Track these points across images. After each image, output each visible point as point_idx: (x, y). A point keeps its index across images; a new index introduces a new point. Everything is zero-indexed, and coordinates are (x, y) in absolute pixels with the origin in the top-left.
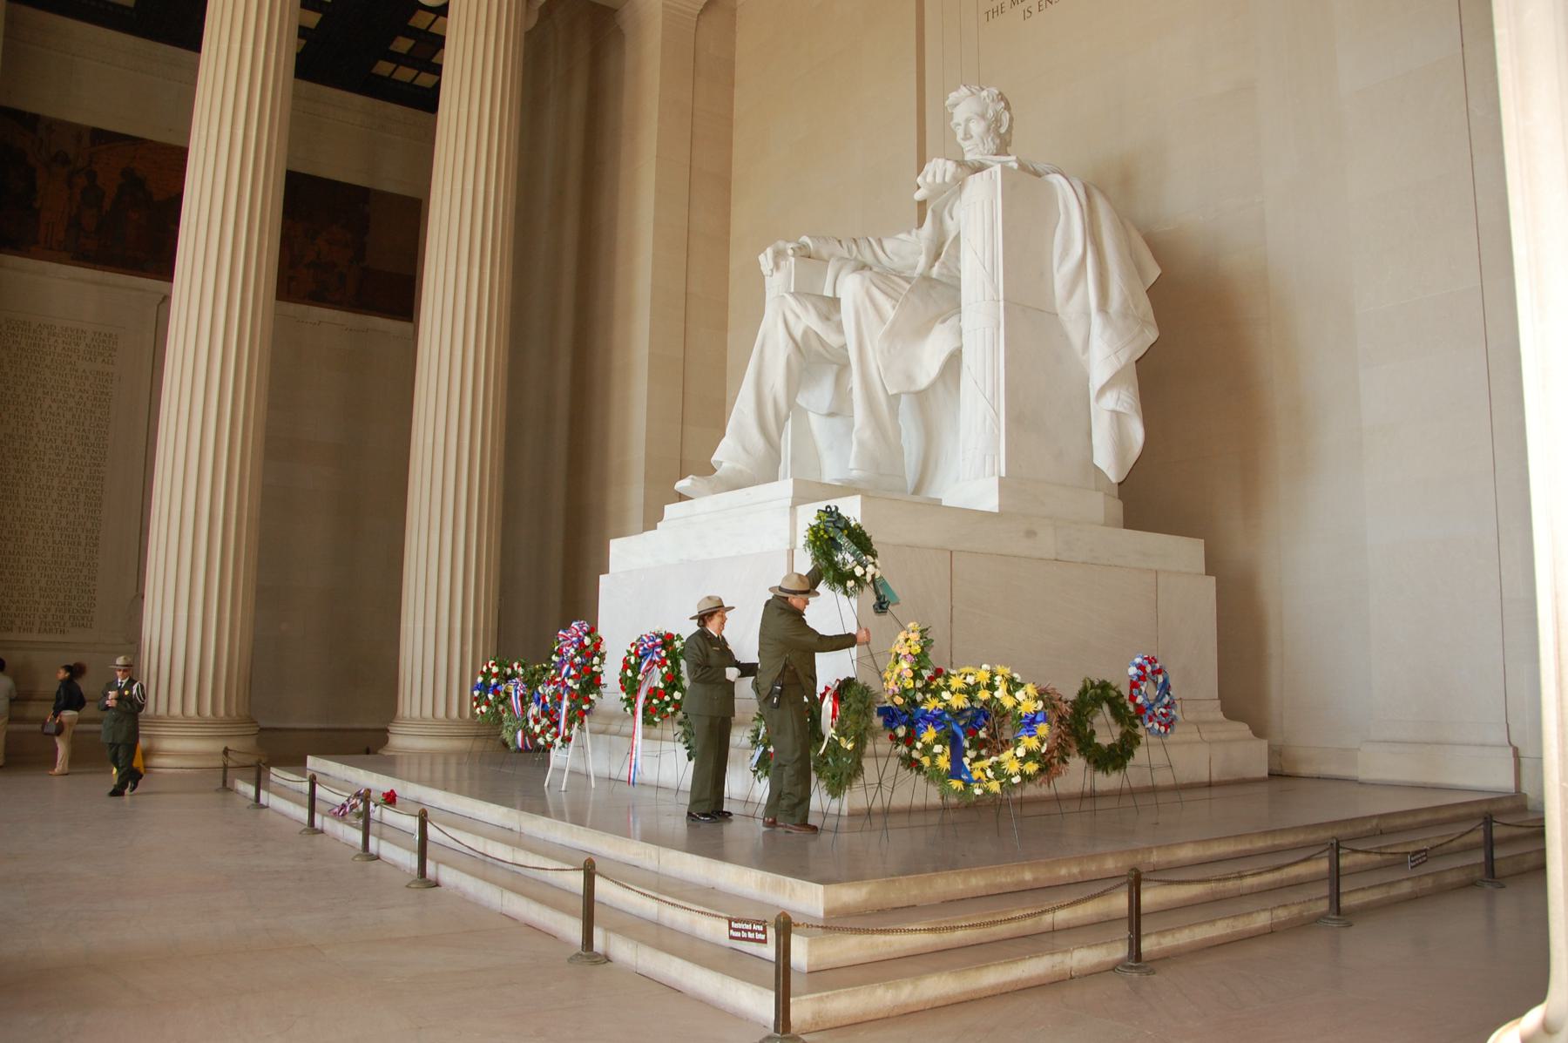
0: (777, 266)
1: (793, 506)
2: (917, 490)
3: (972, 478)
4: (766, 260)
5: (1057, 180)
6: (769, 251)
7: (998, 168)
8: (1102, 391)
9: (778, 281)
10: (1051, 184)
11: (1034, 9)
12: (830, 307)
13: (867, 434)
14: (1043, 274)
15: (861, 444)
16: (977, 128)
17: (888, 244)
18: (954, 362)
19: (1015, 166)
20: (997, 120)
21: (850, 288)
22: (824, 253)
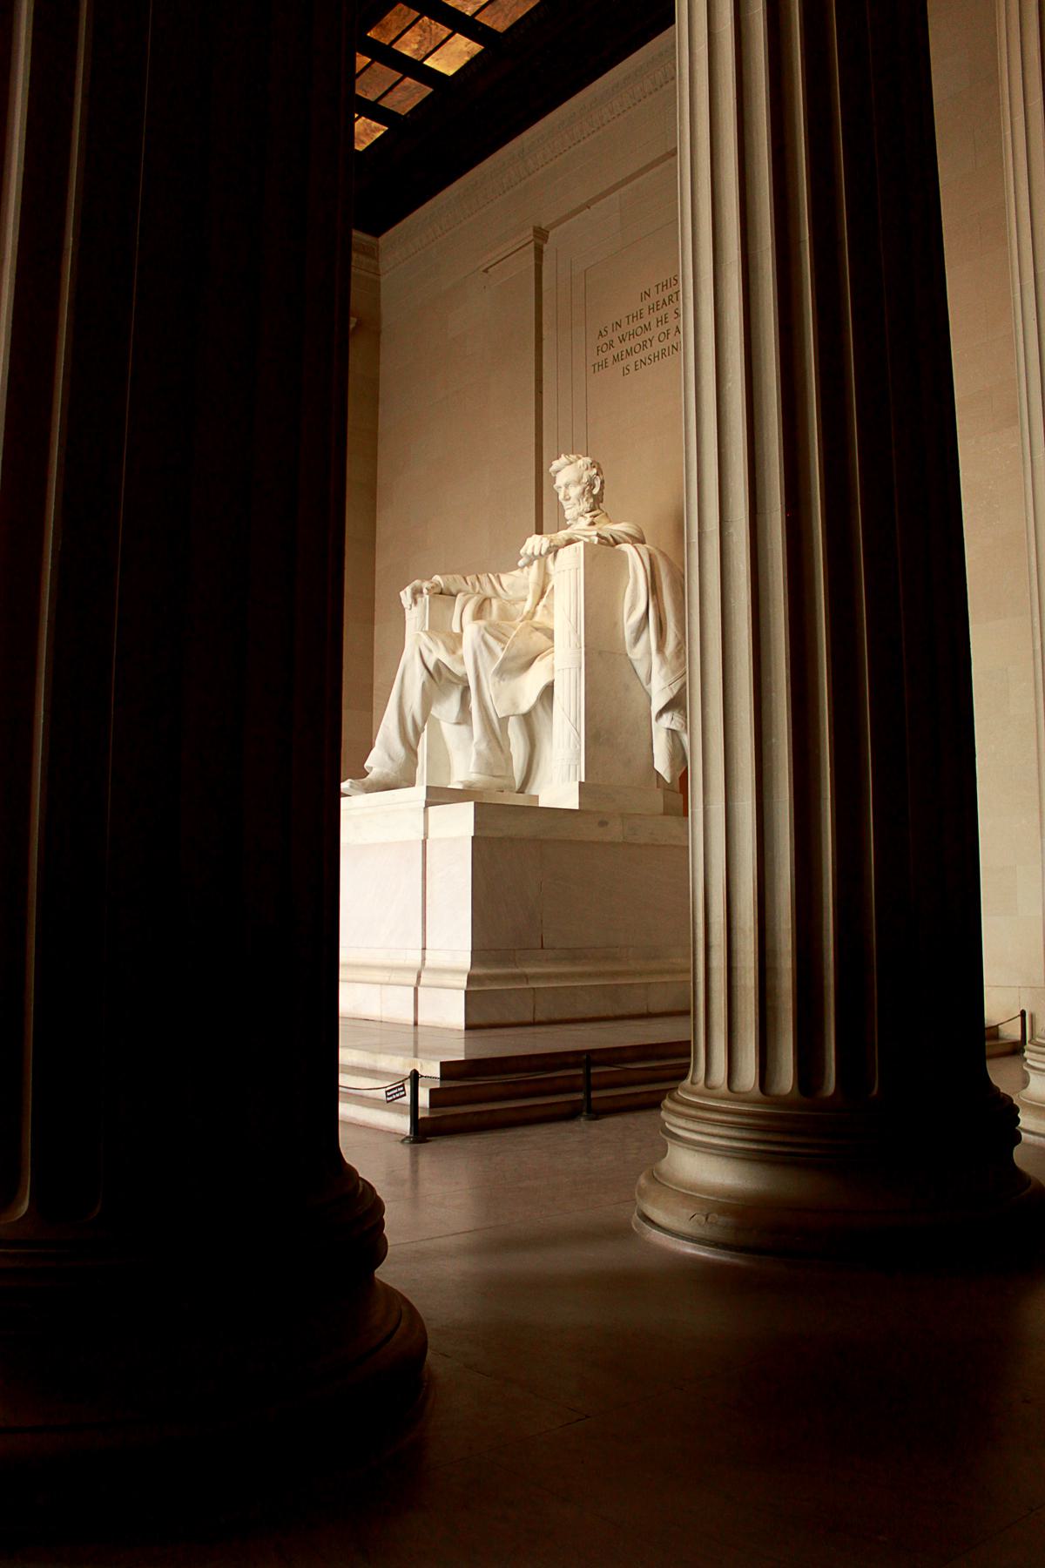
0: (415, 601)
1: (428, 804)
2: (521, 791)
3: (559, 787)
4: (406, 596)
5: (627, 548)
6: (408, 589)
7: (581, 544)
8: (661, 713)
9: (415, 617)
10: (624, 553)
11: (632, 368)
12: (454, 642)
13: (483, 746)
14: (615, 625)
15: (479, 754)
16: (575, 491)
17: (503, 578)
18: (548, 692)
19: (596, 540)
20: (591, 485)
21: (471, 632)
22: (454, 591)
